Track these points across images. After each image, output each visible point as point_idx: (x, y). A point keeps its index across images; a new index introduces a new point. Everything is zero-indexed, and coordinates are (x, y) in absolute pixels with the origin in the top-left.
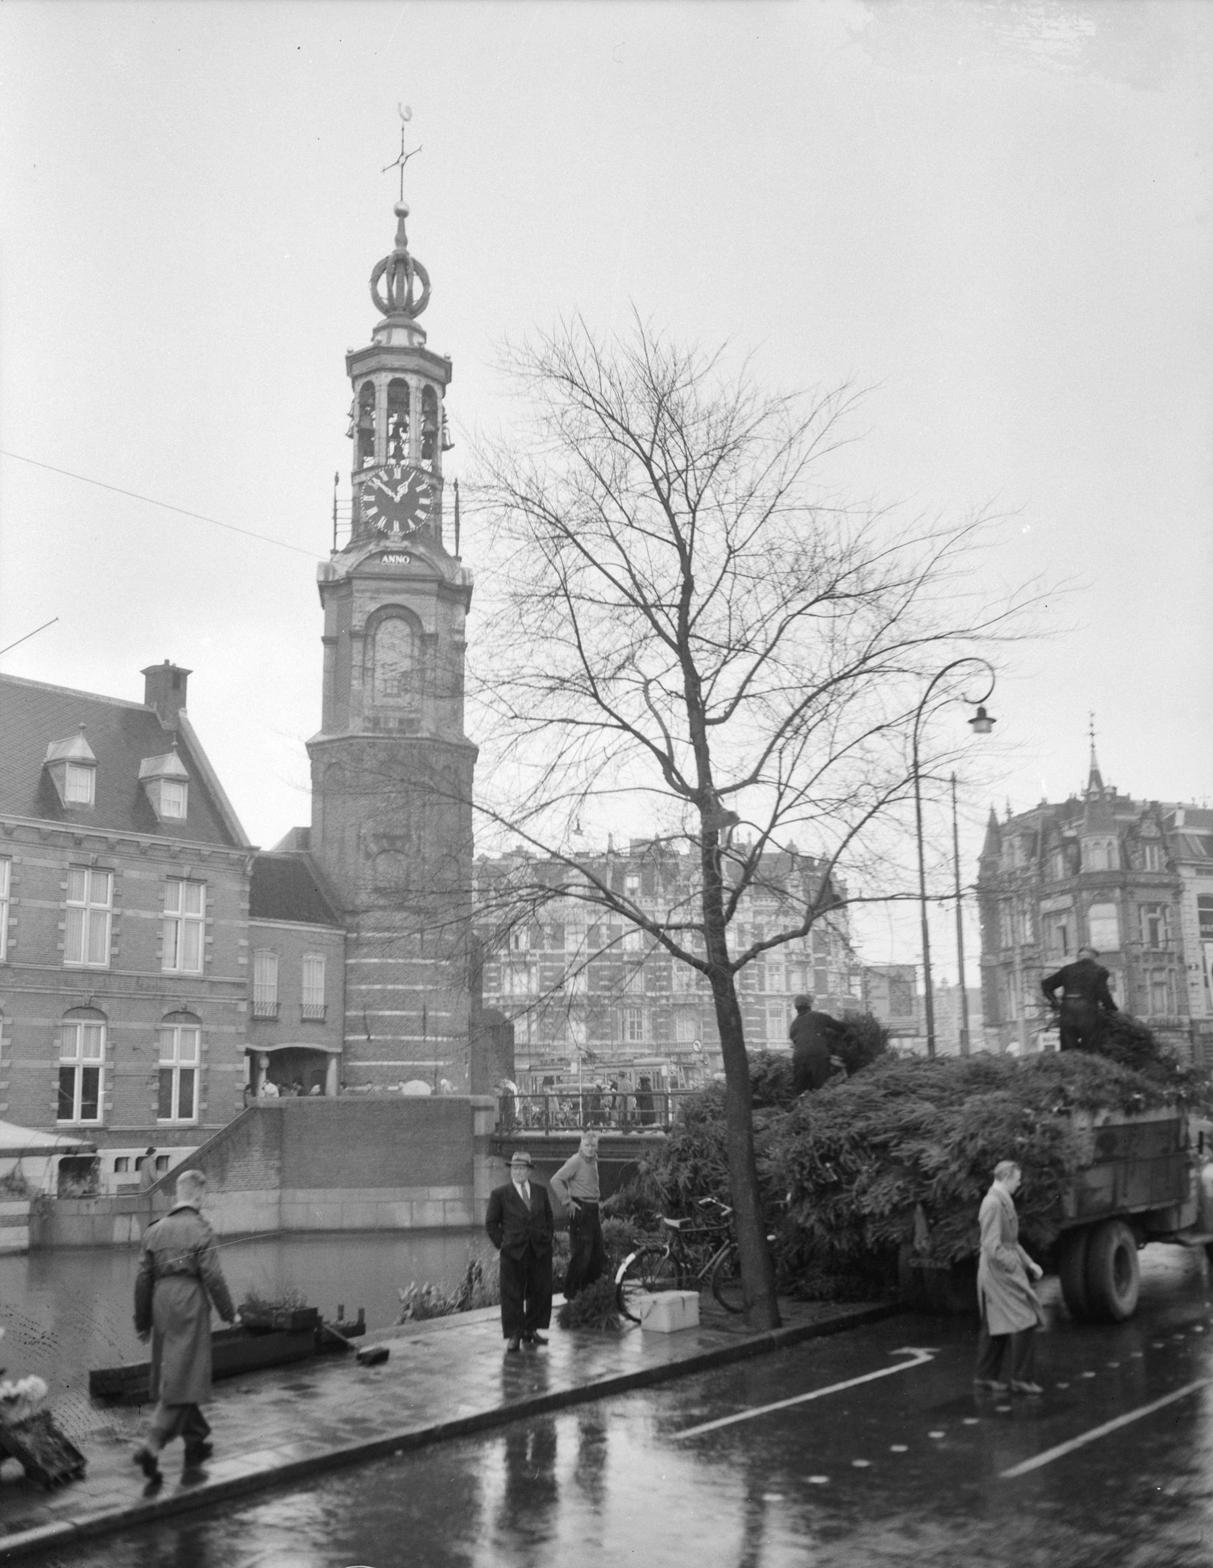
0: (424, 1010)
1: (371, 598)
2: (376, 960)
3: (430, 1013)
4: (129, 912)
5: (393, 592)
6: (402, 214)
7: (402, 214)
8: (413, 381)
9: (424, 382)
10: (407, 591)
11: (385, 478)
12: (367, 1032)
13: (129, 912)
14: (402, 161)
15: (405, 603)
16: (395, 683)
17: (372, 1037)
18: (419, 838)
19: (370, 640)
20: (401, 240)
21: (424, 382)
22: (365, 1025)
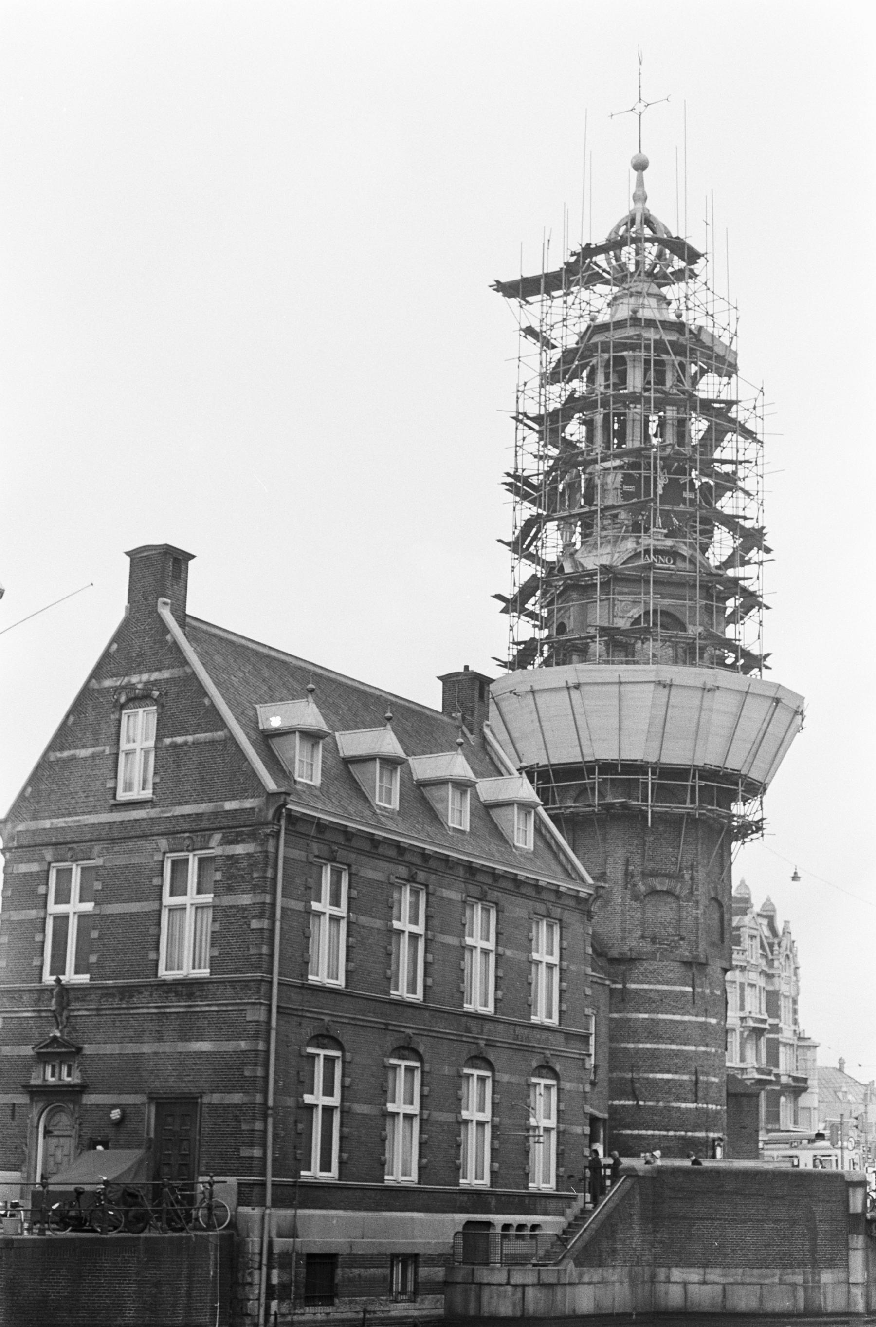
0: (696, 1073)
2: (646, 1016)
3: (701, 1078)
6: (640, 166)
7: (640, 166)
12: (636, 1099)
14: (640, 108)
17: (641, 1103)
20: (640, 197)
22: (630, 1090)
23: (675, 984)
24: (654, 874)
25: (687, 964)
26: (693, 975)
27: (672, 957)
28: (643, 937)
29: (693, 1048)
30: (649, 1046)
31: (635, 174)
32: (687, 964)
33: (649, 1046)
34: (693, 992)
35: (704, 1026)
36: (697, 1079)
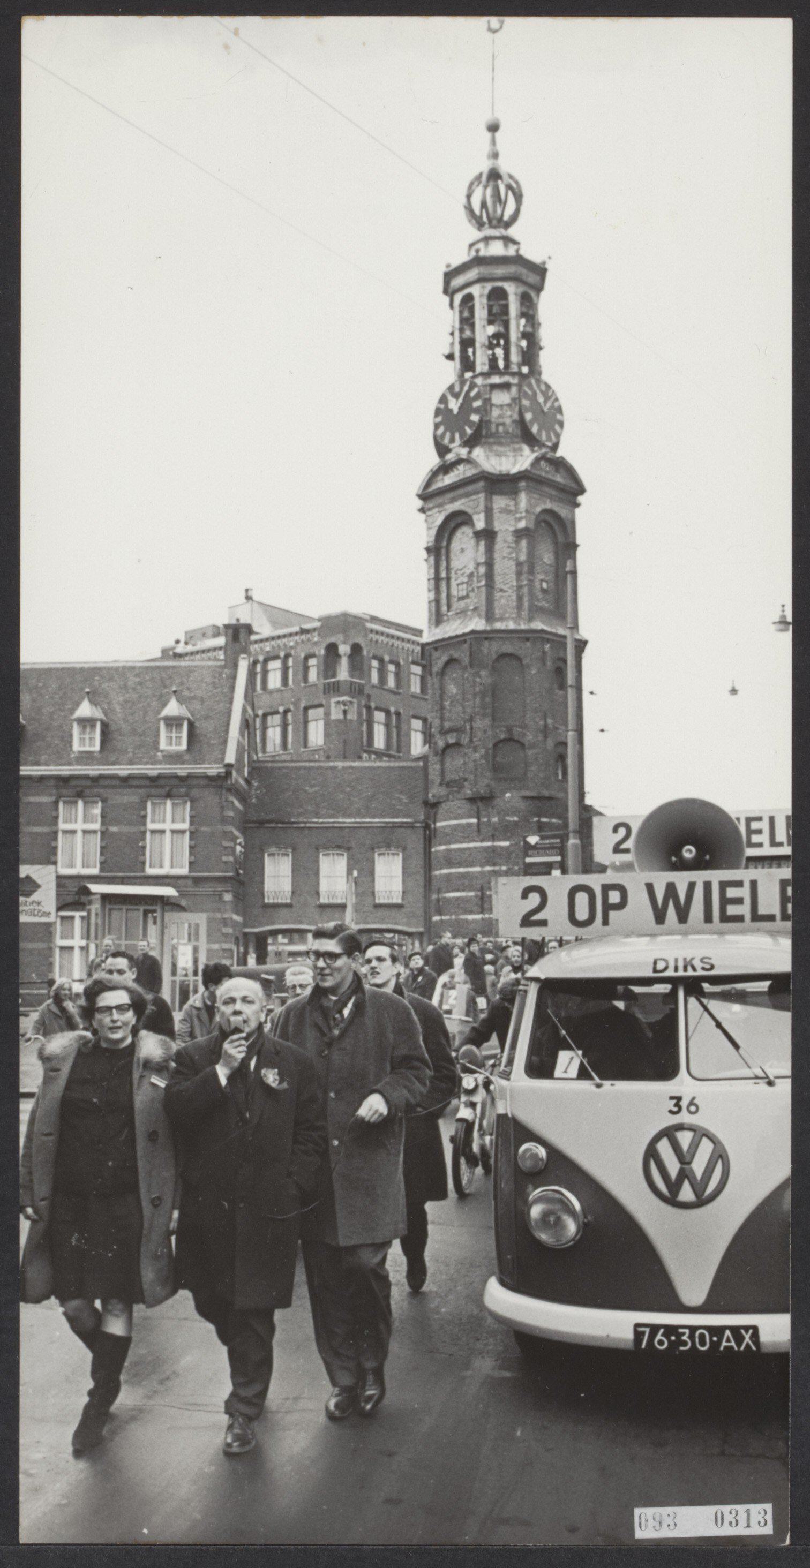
1: (440, 512)
4: (114, 829)
5: (453, 500)
6: (493, 128)
7: (493, 128)
8: (475, 290)
9: (489, 286)
10: (461, 497)
11: (472, 394)
13: (114, 829)
15: (463, 508)
16: (465, 586)
18: (472, 728)
19: (443, 551)
20: (495, 155)
21: (489, 286)
23: (462, 818)
24: (451, 730)
25: (472, 800)
26: (478, 808)
27: (459, 796)
28: (441, 784)
29: (477, 869)
30: (445, 871)
31: (488, 135)
32: (472, 800)
33: (445, 871)
34: (478, 824)
35: (494, 849)
36: (483, 894)
